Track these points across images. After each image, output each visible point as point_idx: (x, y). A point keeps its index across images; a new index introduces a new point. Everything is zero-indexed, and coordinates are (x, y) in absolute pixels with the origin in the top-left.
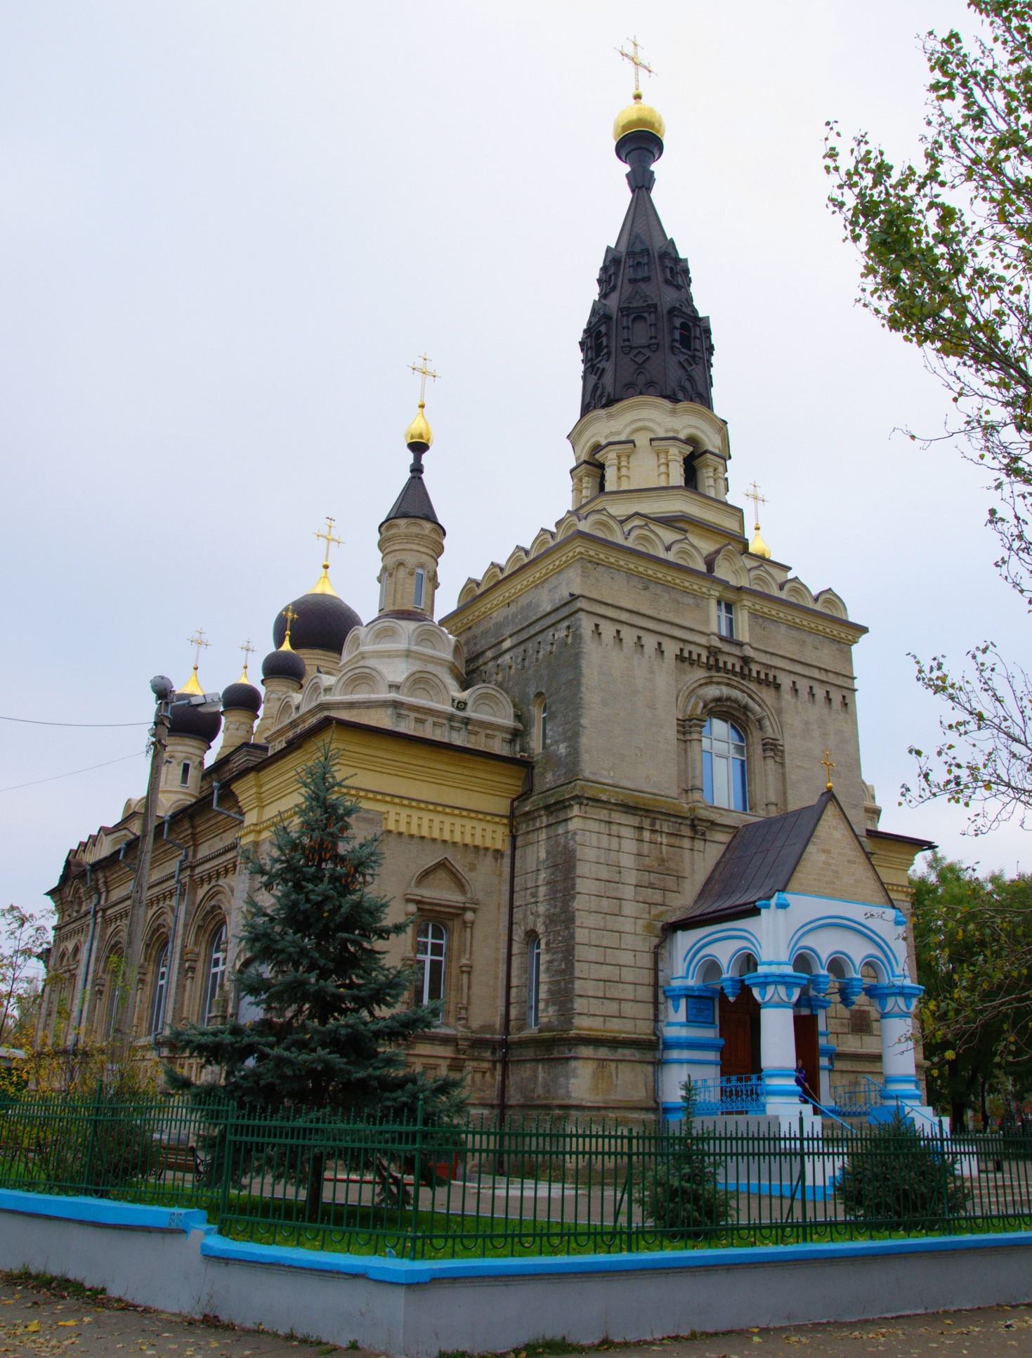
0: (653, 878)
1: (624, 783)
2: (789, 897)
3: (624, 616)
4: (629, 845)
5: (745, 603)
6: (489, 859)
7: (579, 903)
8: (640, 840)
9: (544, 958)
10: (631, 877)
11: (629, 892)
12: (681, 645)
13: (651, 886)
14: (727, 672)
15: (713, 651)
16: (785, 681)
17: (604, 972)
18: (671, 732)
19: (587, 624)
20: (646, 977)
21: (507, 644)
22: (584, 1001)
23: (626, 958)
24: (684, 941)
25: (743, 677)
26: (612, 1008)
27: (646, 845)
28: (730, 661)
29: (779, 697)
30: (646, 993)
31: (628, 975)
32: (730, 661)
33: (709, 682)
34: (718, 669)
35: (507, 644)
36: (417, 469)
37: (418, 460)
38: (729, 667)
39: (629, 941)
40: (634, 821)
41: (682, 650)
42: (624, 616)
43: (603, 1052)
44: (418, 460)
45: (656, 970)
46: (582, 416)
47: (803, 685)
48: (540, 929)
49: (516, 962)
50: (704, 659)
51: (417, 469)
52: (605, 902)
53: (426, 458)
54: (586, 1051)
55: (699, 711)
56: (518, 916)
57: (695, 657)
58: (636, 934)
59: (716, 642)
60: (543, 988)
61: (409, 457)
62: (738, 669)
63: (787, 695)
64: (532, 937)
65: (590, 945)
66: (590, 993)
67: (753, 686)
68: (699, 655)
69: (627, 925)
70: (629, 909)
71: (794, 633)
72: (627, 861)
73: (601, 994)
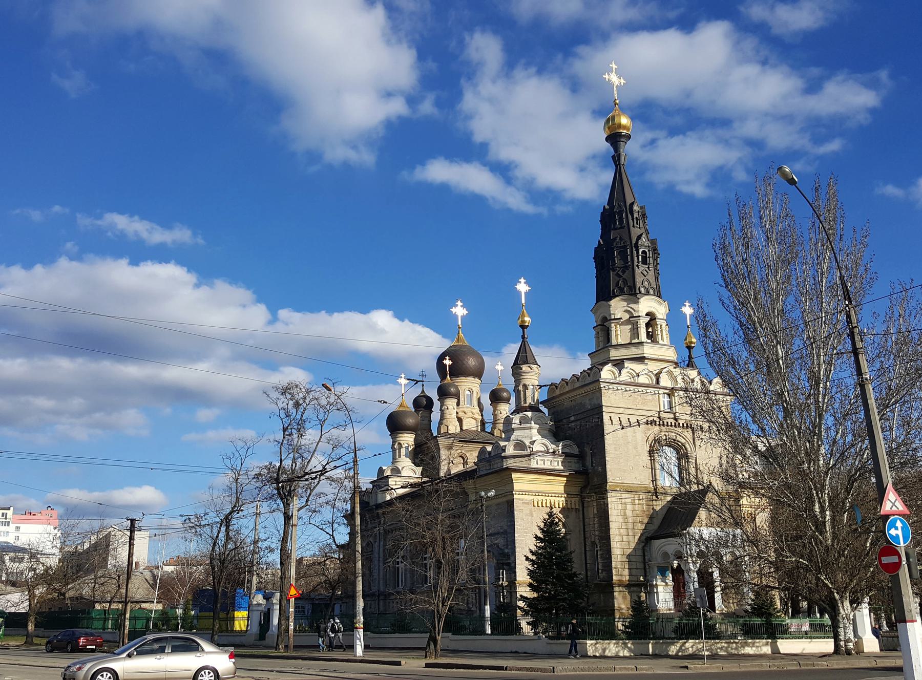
3: (621, 410)
6: (574, 513)
7: (612, 532)
9: (599, 553)
18: (647, 454)
19: (606, 417)
20: (640, 559)
21: (572, 418)
24: (657, 543)
28: (669, 421)
30: (640, 565)
34: (663, 425)
35: (572, 418)
40: (631, 496)
42: (621, 410)
45: (644, 556)
46: (597, 302)
48: (597, 541)
49: (588, 554)
56: (588, 535)
60: (600, 565)
64: (594, 543)
67: (680, 430)
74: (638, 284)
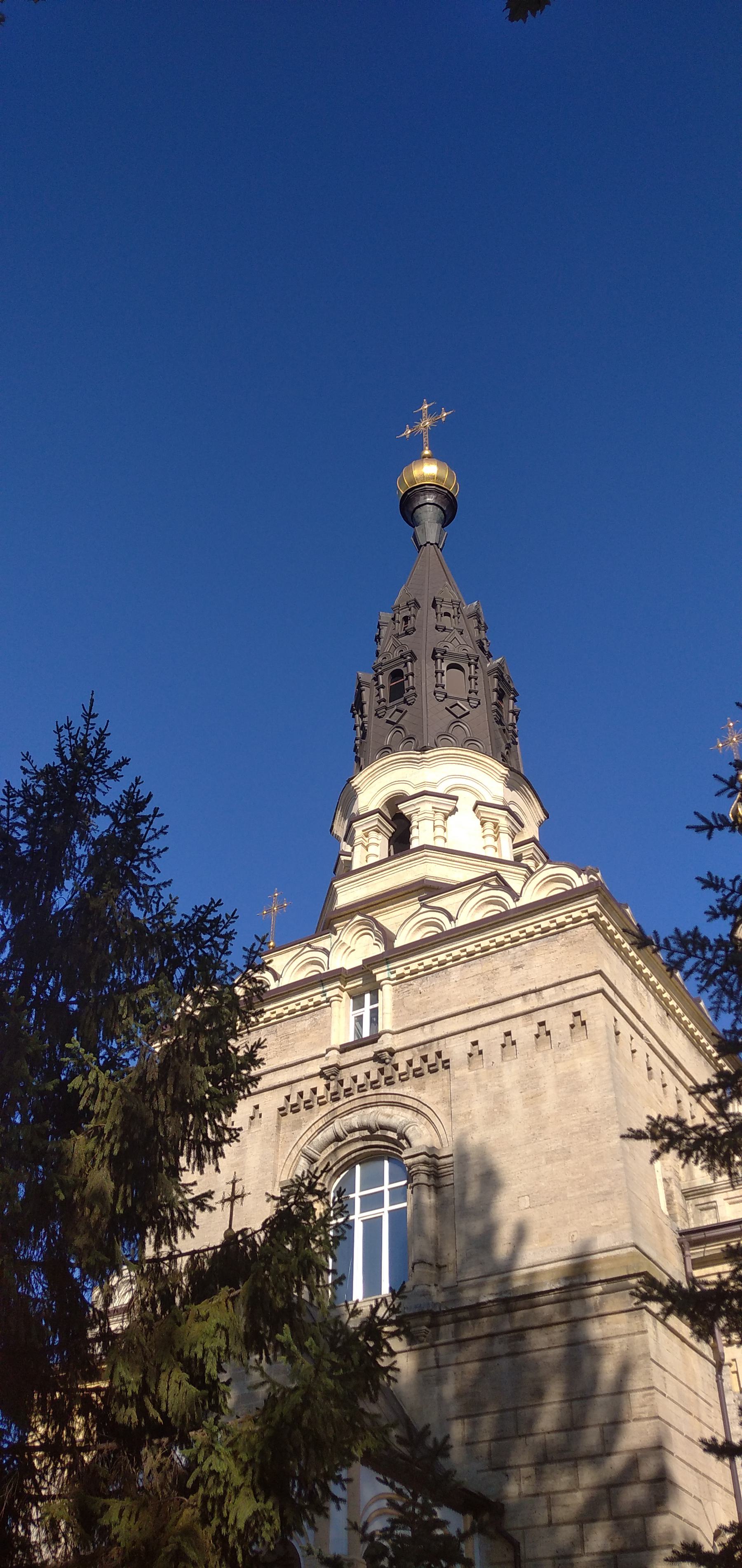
5: (379, 977)
12: (286, 1091)
15: (330, 1073)
16: (457, 1049)
25: (389, 1081)
32: (359, 1072)
41: (288, 1098)
50: (321, 1092)
59: (334, 1058)
63: (460, 1071)
71: (477, 967)
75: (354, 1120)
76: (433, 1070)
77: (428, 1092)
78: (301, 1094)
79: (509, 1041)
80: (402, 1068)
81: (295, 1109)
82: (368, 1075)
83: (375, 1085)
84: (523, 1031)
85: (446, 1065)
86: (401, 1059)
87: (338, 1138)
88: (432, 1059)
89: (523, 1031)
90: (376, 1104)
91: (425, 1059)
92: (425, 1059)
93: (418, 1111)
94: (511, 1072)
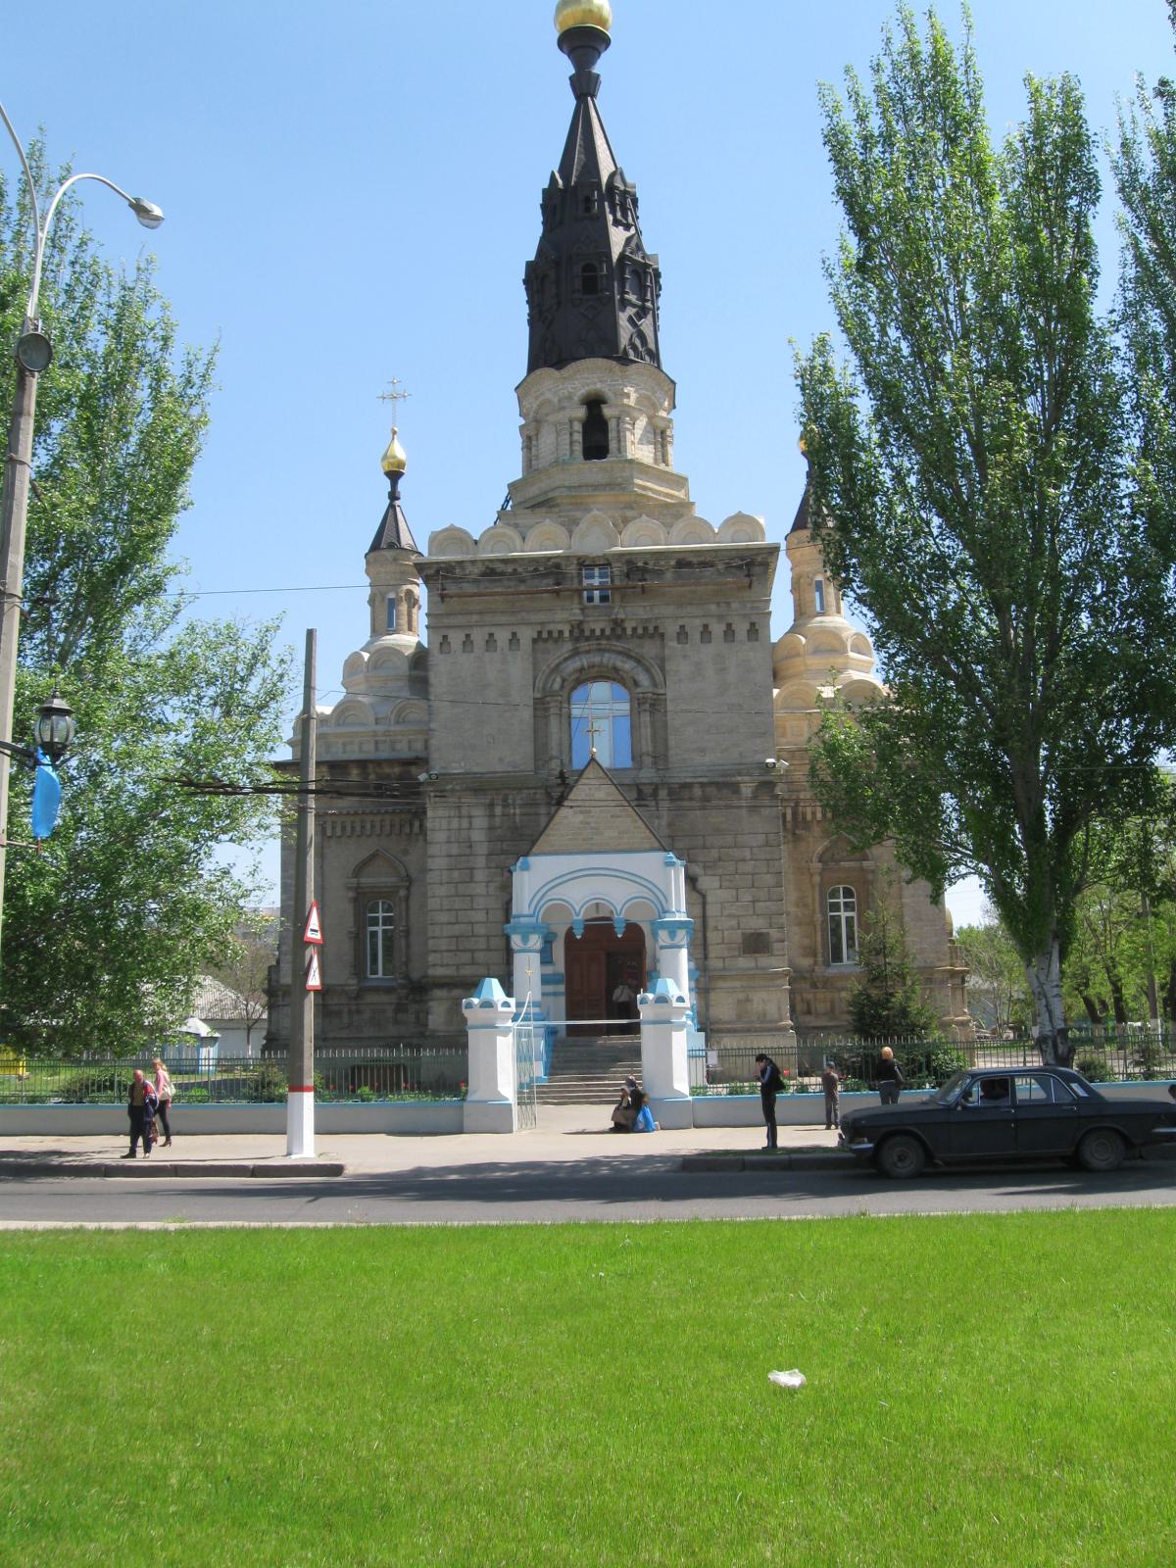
0: (505, 846)
1: (475, 770)
2: (531, 859)
4: (480, 822)
8: (492, 816)
10: (482, 849)
11: (481, 862)
13: (503, 852)
14: (598, 638)
16: (671, 629)
17: (457, 929)
22: (438, 955)
23: (480, 916)
25: (619, 638)
26: (466, 957)
27: (497, 819)
29: (663, 647)
31: (480, 930)
33: (575, 653)
36: (393, 496)
37: (394, 485)
38: (598, 633)
39: (480, 903)
41: (540, 633)
43: (456, 992)
44: (394, 485)
47: (694, 626)
51: (393, 496)
52: (456, 874)
53: (401, 483)
54: (438, 993)
55: (557, 686)
57: (555, 635)
58: (488, 895)
61: (387, 483)
62: (608, 632)
65: (441, 910)
66: (443, 948)
67: (631, 645)
68: (561, 632)
69: (480, 889)
70: (480, 875)
72: (478, 836)
73: (453, 948)
74: (624, 341)
75: (596, 659)
76: (652, 636)
77: (649, 649)
78: (550, 633)
79: (706, 633)
80: (629, 632)
81: (546, 641)
82: (603, 631)
83: (608, 638)
84: (717, 629)
85: (662, 636)
86: (629, 626)
87: (582, 670)
88: (651, 629)
89: (717, 629)
90: (609, 651)
91: (645, 629)
92: (645, 629)
93: (638, 662)
94: (709, 650)
